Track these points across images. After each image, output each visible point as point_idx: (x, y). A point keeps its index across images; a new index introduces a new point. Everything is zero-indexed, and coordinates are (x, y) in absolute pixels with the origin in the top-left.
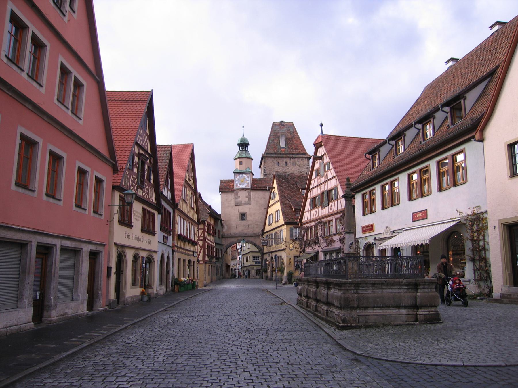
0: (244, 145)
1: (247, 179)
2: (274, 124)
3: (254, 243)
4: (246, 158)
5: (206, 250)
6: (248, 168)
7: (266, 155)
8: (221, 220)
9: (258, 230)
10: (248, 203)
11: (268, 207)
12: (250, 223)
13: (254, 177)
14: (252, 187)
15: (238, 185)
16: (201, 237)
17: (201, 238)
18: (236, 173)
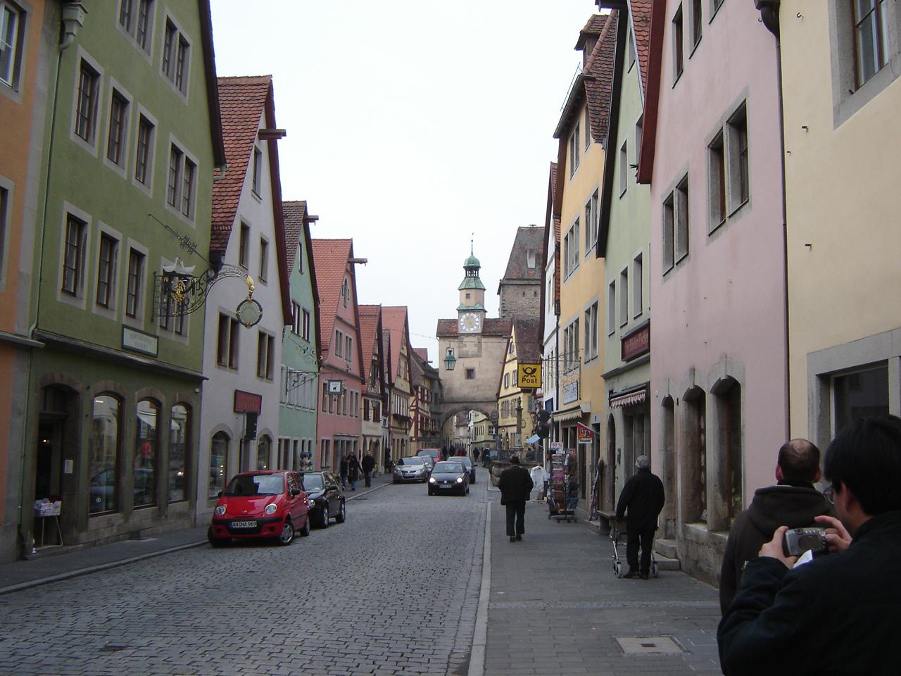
0: (472, 268)
1: (477, 320)
2: (520, 230)
3: (485, 411)
4: (476, 289)
5: (419, 424)
6: (479, 303)
7: (506, 282)
8: (439, 380)
9: (491, 394)
10: (478, 355)
11: (505, 363)
12: (480, 382)
13: (489, 316)
14: (483, 332)
15: (463, 328)
16: (412, 406)
17: (412, 408)
18: (461, 311)
